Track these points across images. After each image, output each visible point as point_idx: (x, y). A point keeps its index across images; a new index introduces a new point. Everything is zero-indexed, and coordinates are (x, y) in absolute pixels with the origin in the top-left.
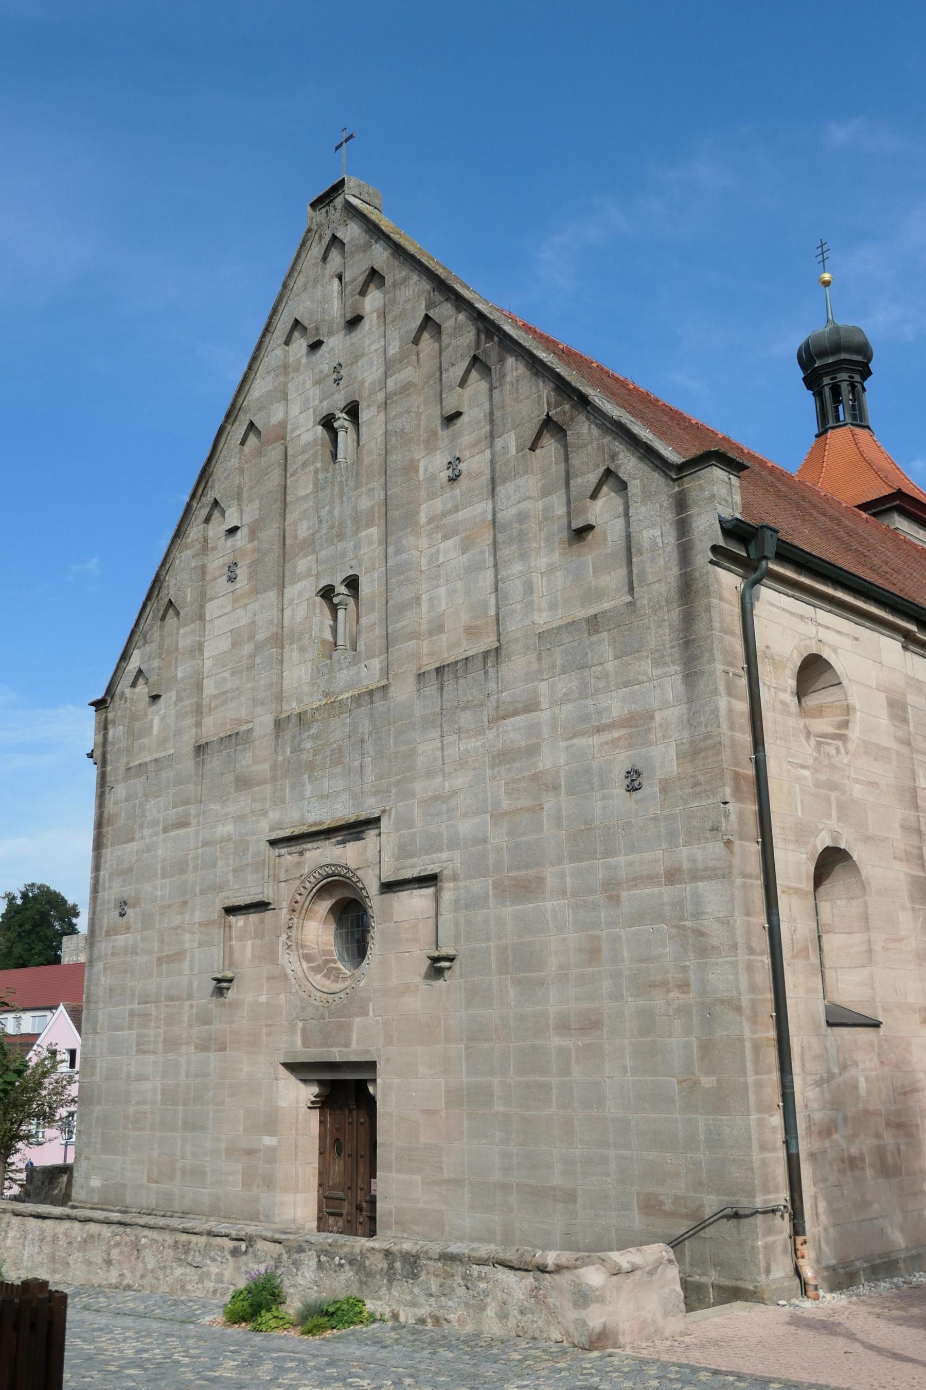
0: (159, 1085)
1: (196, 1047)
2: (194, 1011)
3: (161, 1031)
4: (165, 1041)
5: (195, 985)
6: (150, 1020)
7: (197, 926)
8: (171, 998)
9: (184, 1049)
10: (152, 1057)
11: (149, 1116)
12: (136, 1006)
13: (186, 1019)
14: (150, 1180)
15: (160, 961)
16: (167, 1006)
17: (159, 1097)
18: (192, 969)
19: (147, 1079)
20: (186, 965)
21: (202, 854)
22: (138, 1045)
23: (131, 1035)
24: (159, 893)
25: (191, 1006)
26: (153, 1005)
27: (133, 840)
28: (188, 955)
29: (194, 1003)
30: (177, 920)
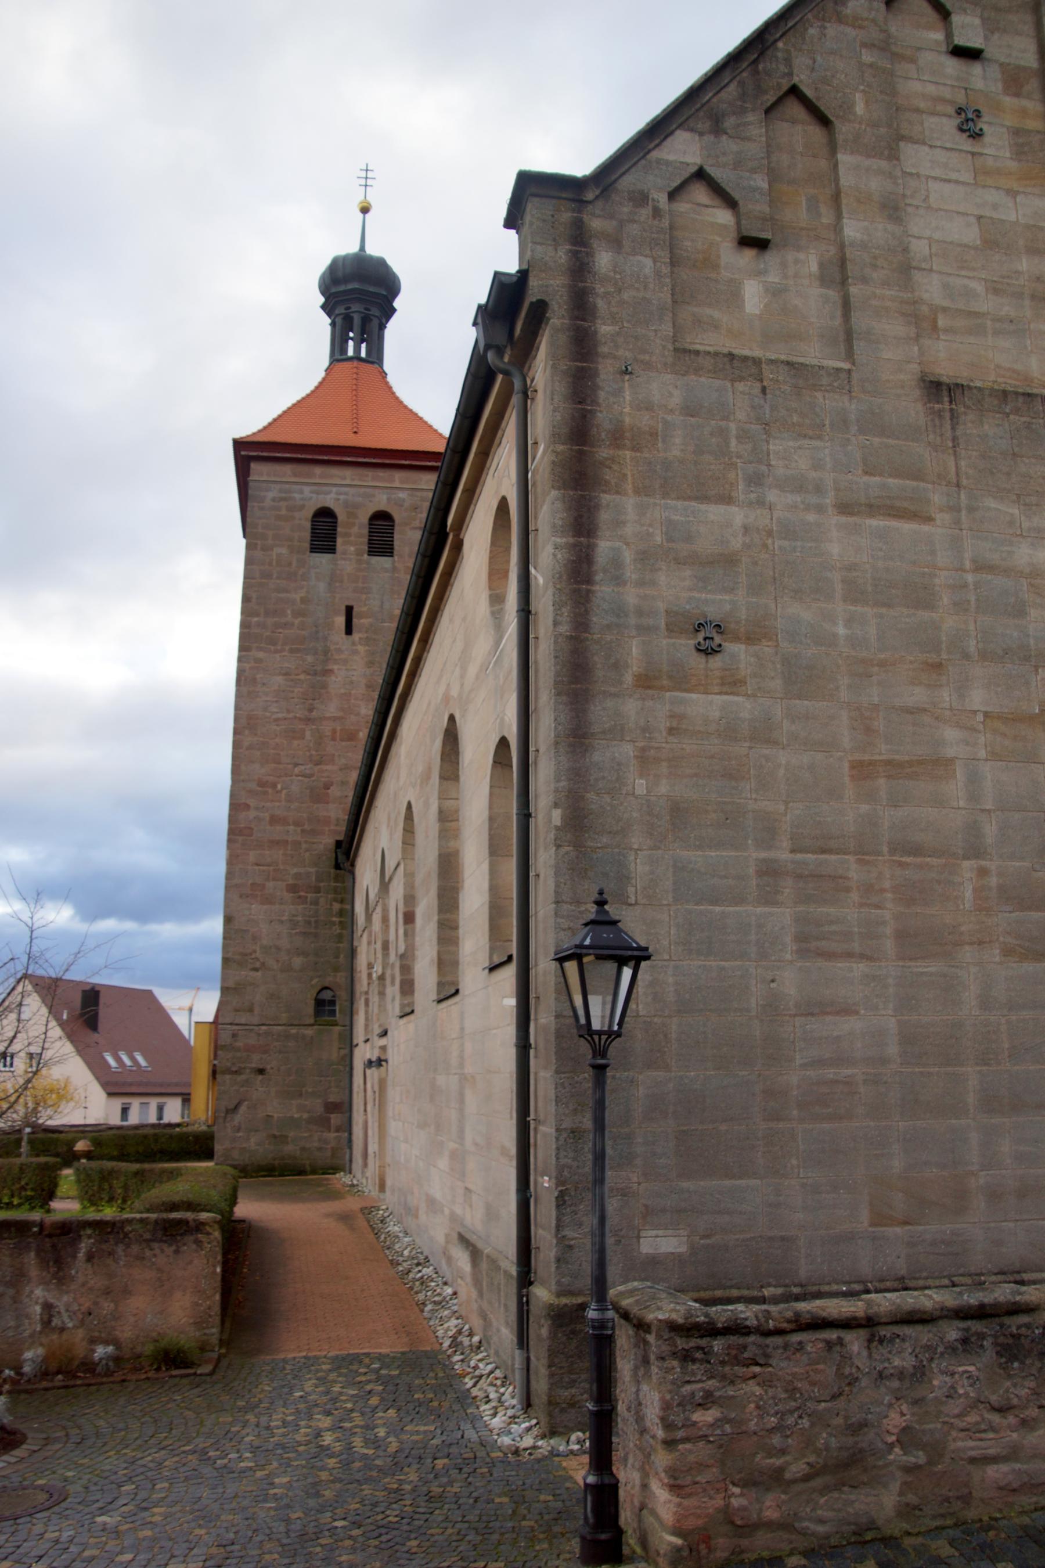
0: (892, 1024)
1: (1008, 952)
2: (994, 881)
3: (887, 915)
4: (902, 936)
5: (990, 831)
6: (848, 890)
7: (980, 717)
8: (907, 848)
9: (968, 954)
10: (860, 968)
11: (862, 1089)
12: (783, 855)
13: (969, 894)
14: (879, 1219)
15: (863, 771)
16: (901, 864)
17: (893, 1049)
18: (974, 797)
19: (847, 1010)
20: (956, 789)
21: (977, 585)
22: (801, 938)
23: (782, 918)
24: (841, 631)
25: (983, 872)
26: (851, 858)
27: (727, 499)
28: (959, 774)
29: (992, 865)
30: (917, 696)
